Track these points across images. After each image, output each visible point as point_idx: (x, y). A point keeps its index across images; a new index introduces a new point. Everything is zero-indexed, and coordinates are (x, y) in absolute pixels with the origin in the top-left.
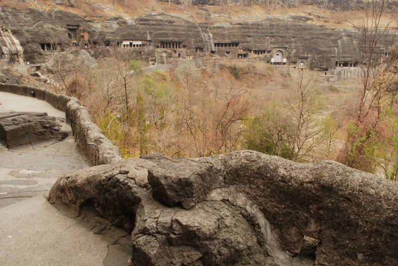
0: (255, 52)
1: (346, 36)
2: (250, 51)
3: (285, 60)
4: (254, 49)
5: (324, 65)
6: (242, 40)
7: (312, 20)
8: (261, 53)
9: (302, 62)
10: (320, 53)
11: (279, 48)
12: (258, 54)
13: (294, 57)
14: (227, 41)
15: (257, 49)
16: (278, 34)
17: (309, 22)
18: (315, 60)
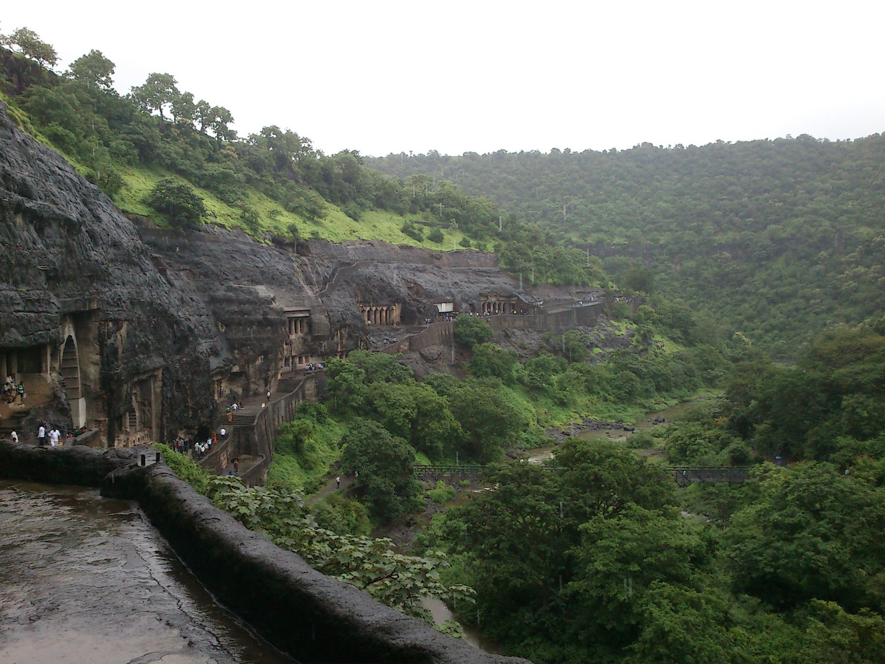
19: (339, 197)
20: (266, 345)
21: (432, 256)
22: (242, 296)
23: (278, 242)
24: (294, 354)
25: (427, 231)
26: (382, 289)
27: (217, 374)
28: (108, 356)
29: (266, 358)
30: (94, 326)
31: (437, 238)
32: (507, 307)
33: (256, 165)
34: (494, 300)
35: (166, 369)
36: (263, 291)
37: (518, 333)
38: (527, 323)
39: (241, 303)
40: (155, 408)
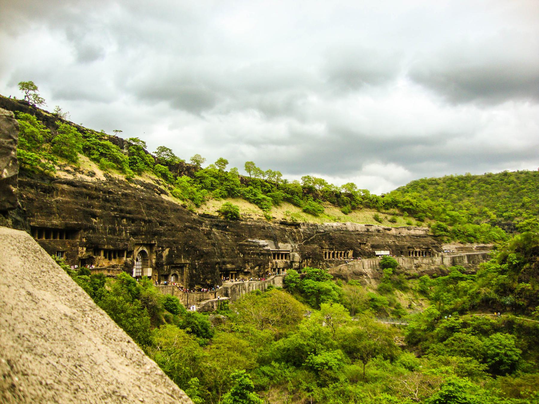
0: (110, 254)
1: (212, 226)
2: (97, 251)
3: (149, 272)
4: (106, 247)
5: (208, 280)
6: (85, 222)
7: (166, 194)
8: (115, 258)
9: (172, 275)
10: (202, 255)
11: (141, 245)
12: (110, 259)
13: (167, 265)
14: (56, 222)
16: (140, 216)
17: (163, 196)
18: (196, 269)
20: (259, 262)
21: (385, 229)
22: (252, 243)
24: (278, 267)
25: (390, 217)
26: (342, 244)
27: (232, 271)
28: (160, 257)
29: (260, 268)
30: (155, 249)
31: (393, 221)
32: (427, 253)
33: (292, 193)
34: (418, 250)
36: (262, 242)
37: (423, 265)
38: (431, 261)
39: (251, 246)
40: (185, 276)
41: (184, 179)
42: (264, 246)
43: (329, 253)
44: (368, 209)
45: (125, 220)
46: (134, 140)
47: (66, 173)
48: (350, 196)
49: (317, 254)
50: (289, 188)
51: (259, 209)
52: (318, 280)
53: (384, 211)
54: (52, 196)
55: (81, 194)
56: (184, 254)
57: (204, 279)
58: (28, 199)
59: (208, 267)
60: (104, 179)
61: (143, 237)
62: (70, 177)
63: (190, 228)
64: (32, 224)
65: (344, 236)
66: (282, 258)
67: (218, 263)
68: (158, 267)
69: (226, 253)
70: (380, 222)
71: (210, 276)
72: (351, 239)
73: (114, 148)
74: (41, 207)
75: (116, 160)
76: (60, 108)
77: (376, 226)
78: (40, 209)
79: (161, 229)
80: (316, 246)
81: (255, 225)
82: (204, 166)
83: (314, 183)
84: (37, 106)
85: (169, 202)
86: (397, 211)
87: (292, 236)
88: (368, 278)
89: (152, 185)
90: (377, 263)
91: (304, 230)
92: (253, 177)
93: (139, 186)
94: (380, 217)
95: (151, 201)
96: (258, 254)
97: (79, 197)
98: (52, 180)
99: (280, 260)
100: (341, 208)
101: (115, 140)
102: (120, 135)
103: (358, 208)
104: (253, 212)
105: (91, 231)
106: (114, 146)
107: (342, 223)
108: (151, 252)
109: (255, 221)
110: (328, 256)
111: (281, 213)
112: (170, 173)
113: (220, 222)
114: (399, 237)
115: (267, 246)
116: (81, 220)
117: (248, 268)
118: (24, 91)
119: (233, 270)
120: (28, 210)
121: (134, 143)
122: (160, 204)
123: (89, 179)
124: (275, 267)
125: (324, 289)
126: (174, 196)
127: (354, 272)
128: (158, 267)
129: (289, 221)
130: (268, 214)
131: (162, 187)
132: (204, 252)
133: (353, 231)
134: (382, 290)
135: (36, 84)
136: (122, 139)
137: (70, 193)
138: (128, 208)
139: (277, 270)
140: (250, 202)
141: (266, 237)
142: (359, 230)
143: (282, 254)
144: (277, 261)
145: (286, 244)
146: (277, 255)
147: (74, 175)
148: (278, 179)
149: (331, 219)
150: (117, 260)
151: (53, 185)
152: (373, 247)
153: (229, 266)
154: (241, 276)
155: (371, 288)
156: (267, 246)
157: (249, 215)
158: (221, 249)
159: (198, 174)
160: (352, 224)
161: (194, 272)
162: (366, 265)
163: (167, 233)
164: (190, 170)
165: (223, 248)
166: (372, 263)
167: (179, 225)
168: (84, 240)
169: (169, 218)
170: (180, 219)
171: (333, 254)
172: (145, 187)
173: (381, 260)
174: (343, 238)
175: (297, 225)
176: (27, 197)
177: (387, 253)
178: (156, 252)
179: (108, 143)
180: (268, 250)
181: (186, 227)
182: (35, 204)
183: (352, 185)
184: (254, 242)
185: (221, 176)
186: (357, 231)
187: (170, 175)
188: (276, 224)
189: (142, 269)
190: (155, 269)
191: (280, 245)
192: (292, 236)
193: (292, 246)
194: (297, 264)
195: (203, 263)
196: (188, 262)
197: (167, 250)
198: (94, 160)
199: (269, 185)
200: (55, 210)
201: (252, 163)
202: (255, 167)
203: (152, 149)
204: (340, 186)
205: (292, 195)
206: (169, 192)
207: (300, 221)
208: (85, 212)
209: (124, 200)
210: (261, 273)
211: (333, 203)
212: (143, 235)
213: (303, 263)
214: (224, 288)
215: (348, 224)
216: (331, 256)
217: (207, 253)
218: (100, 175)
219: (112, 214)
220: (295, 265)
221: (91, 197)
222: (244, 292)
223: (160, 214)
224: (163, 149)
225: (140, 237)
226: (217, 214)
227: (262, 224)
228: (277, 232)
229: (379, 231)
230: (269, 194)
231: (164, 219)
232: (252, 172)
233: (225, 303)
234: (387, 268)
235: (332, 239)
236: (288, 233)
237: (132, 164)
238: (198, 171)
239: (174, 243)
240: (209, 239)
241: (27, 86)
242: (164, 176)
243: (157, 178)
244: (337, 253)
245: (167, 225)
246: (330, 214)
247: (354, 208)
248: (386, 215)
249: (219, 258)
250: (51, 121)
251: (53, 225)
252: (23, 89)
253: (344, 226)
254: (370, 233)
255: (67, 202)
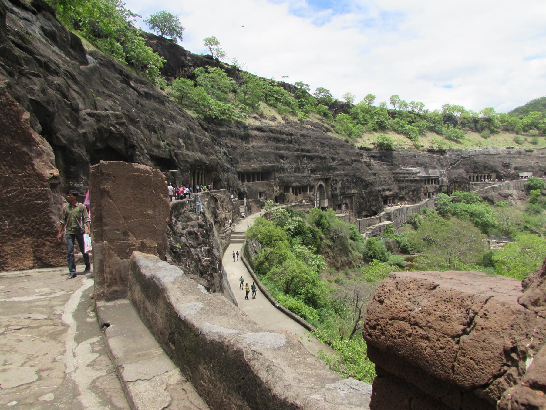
3: (326, 203)
4: (294, 184)
5: (373, 206)
6: (277, 164)
7: (330, 131)
8: (300, 193)
10: (367, 185)
11: (319, 180)
13: (340, 195)
14: (255, 166)
15: (298, 184)
16: (317, 154)
17: (329, 134)
19: (477, 130)
20: (413, 188)
21: (527, 151)
22: (405, 171)
23: (431, 151)
25: (530, 139)
26: (485, 167)
30: (331, 182)
31: (534, 143)
35: (358, 194)
36: (415, 169)
39: (405, 174)
41: (342, 116)
42: (417, 173)
43: (473, 177)
44: (507, 133)
45: (305, 158)
46: (298, 84)
47: (254, 120)
48: (489, 120)
49: (464, 178)
50: (431, 118)
51: (407, 139)
52: (468, 202)
53: (523, 133)
54: (248, 142)
55: (269, 138)
56: (353, 185)
57: (370, 207)
58: (232, 147)
59: (372, 196)
60: (283, 122)
61: (321, 172)
62: (258, 123)
63: (356, 161)
64: (238, 170)
65: (488, 160)
66: (432, 183)
67: (379, 191)
68: (333, 198)
69: (384, 181)
70: (521, 144)
71: (374, 204)
72: (494, 162)
73: (286, 93)
74: (243, 153)
75: (288, 104)
76: (237, 59)
77: (517, 147)
78: (242, 155)
79: (334, 164)
80: (462, 170)
81: (406, 154)
82: (355, 103)
83: (453, 111)
84: (220, 59)
85: (336, 139)
86: (536, 132)
87: (440, 162)
88: (514, 199)
89: (319, 124)
90: (522, 185)
91: (450, 156)
92: (397, 109)
93: (309, 126)
94: (520, 139)
95: (323, 139)
96: (411, 181)
97: (269, 141)
98: (245, 127)
99: (430, 185)
100: (480, 132)
101: (284, 85)
102: (287, 81)
103: (497, 131)
104: (403, 141)
105: (281, 171)
106: (286, 91)
107: (483, 147)
108: (326, 185)
109: (406, 151)
110: (472, 179)
111: (428, 141)
112: (329, 112)
113: (376, 153)
114: (542, 158)
115: (419, 173)
116: (274, 162)
117: (402, 194)
118: (208, 47)
119: (391, 196)
120: (234, 158)
121: (298, 87)
122: (330, 141)
123: (272, 123)
124: (426, 192)
125: (478, 212)
126: (337, 132)
127: (499, 194)
128: (333, 198)
129: (435, 148)
130: (416, 143)
131: (326, 125)
132: (369, 182)
133: (495, 155)
134: (530, 210)
135: (218, 39)
136: (288, 84)
137: (260, 138)
138: (307, 148)
139: (428, 195)
140: (398, 133)
141: (418, 165)
142: (501, 152)
143: (432, 180)
144: (428, 186)
145: (436, 170)
146: (428, 180)
147: (260, 121)
148: (420, 110)
149: (472, 144)
150: (302, 194)
151: (246, 132)
152: (516, 169)
153: (387, 193)
154: (396, 201)
155: (518, 209)
156: (419, 173)
157: (400, 145)
158: (380, 178)
159: (352, 111)
160: (493, 148)
161: (362, 201)
162: (510, 188)
163: (338, 167)
164: (344, 108)
165: (381, 176)
166: (517, 185)
167: (347, 159)
168: (278, 180)
169: (338, 154)
170: (347, 153)
171: (477, 177)
172: (314, 127)
173: (527, 181)
174: (487, 162)
175: (442, 152)
176: (232, 146)
177: (531, 174)
178: (331, 185)
179: (280, 88)
180: (421, 177)
181: (353, 161)
182: (238, 151)
183: (491, 109)
184: (407, 170)
185: (370, 111)
186: (499, 154)
187: (330, 113)
188: (425, 152)
189: (320, 200)
190: (331, 200)
191: (430, 171)
192: (440, 162)
193: (440, 172)
194: (446, 188)
195: (369, 192)
196: (357, 192)
197: (340, 183)
198: (270, 105)
199: (413, 116)
200: (253, 155)
201: (397, 97)
202: (399, 100)
203: (312, 92)
204: (477, 112)
205: (434, 123)
206: (332, 129)
207: (445, 148)
208: (276, 154)
209: (302, 140)
210: (414, 198)
211: (472, 129)
212: (320, 171)
213: (451, 187)
214: (387, 213)
215: (490, 147)
216: (475, 179)
217: (371, 184)
218: (279, 118)
219: (296, 153)
220: (444, 189)
221: (277, 140)
222: (403, 216)
223: (331, 150)
224: (321, 90)
225: (318, 173)
226: (372, 146)
227: (412, 153)
228: (427, 160)
229: (520, 153)
230: (413, 124)
231: (335, 155)
232: (397, 105)
233: (390, 227)
234: (535, 189)
235: (476, 163)
236: (436, 160)
237: (301, 105)
238: (351, 108)
239: (345, 176)
240: (371, 169)
241: (211, 42)
242: (325, 115)
243: (321, 118)
244: (481, 176)
245: (338, 160)
246: (471, 139)
247: (492, 132)
248: (525, 137)
249: (379, 186)
250: (233, 72)
251: (253, 169)
252: (207, 45)
253: (487, 150)
254: (512, 156)
255: (261, 147)
